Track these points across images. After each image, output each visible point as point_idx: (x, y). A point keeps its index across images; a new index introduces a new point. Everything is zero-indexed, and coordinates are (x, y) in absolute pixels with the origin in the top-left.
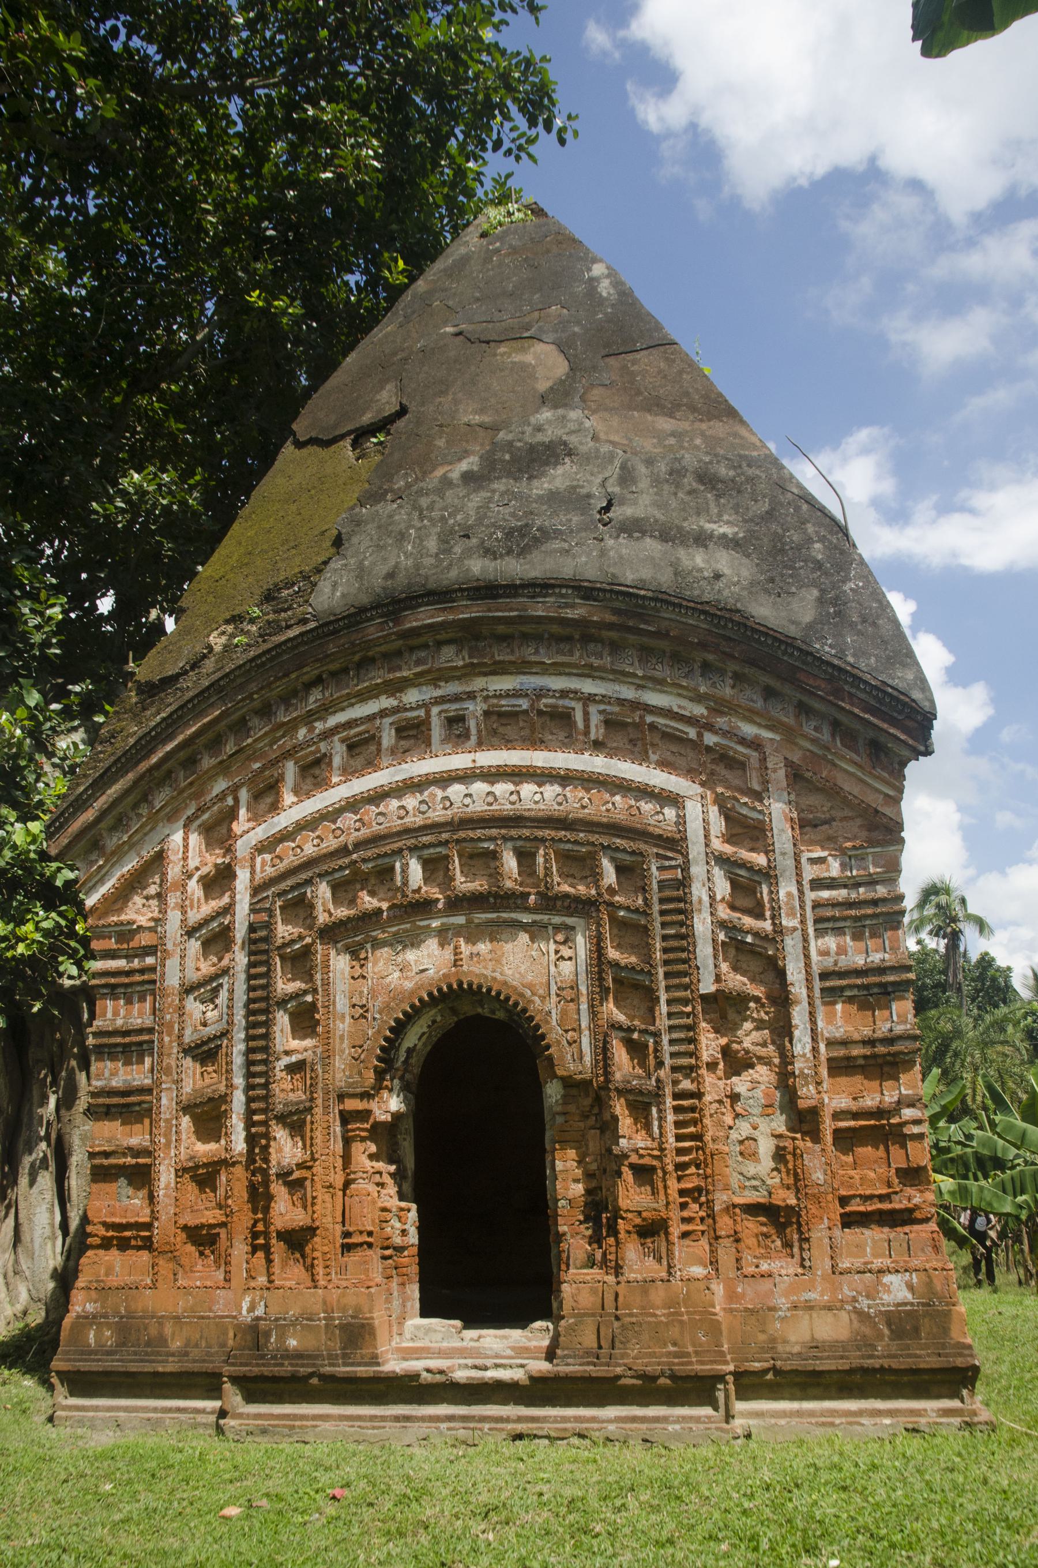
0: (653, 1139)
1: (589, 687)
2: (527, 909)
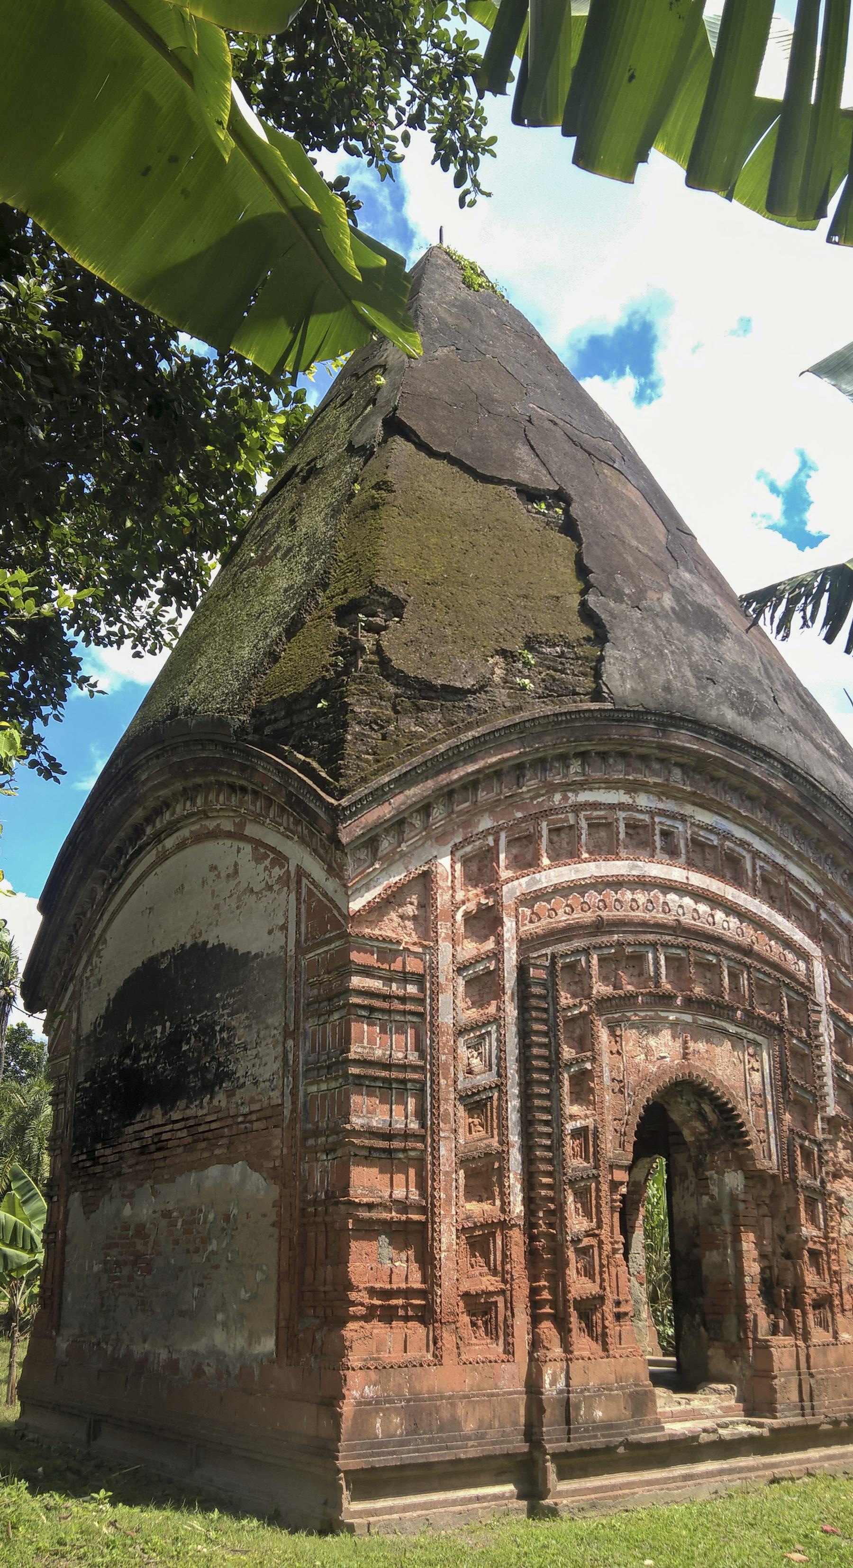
0: (820, 1229)
1: (758, 844)
2: (733, 1021)
